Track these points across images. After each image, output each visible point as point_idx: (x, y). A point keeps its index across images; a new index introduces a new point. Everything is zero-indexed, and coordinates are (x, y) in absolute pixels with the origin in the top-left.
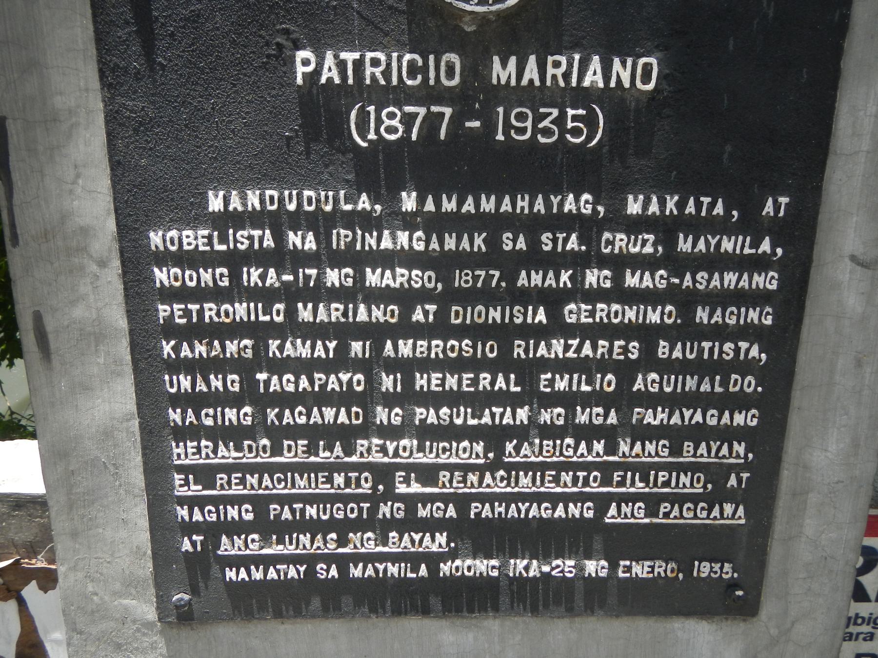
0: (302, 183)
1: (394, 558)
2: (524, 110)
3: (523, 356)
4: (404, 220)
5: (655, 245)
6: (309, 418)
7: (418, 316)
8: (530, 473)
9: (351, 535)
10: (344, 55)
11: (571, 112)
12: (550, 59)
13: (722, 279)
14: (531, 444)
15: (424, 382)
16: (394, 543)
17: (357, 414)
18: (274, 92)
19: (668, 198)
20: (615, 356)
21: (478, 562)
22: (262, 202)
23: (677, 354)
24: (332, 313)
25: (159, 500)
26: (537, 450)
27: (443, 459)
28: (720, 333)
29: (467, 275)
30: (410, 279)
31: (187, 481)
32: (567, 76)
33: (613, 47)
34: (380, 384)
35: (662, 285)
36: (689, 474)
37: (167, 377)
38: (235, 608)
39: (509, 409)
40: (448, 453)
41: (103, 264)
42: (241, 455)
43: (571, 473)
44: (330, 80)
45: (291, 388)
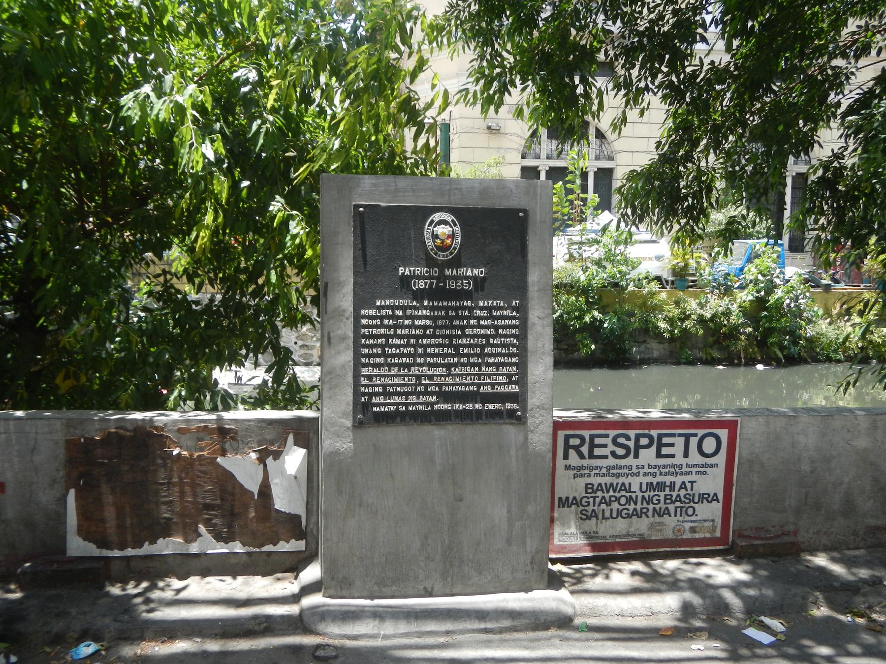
7: (428, 332)
24: (407, 331)
25: (357, 385)
28: (506, 336)
33: (473, 267)
41: (347, 319)
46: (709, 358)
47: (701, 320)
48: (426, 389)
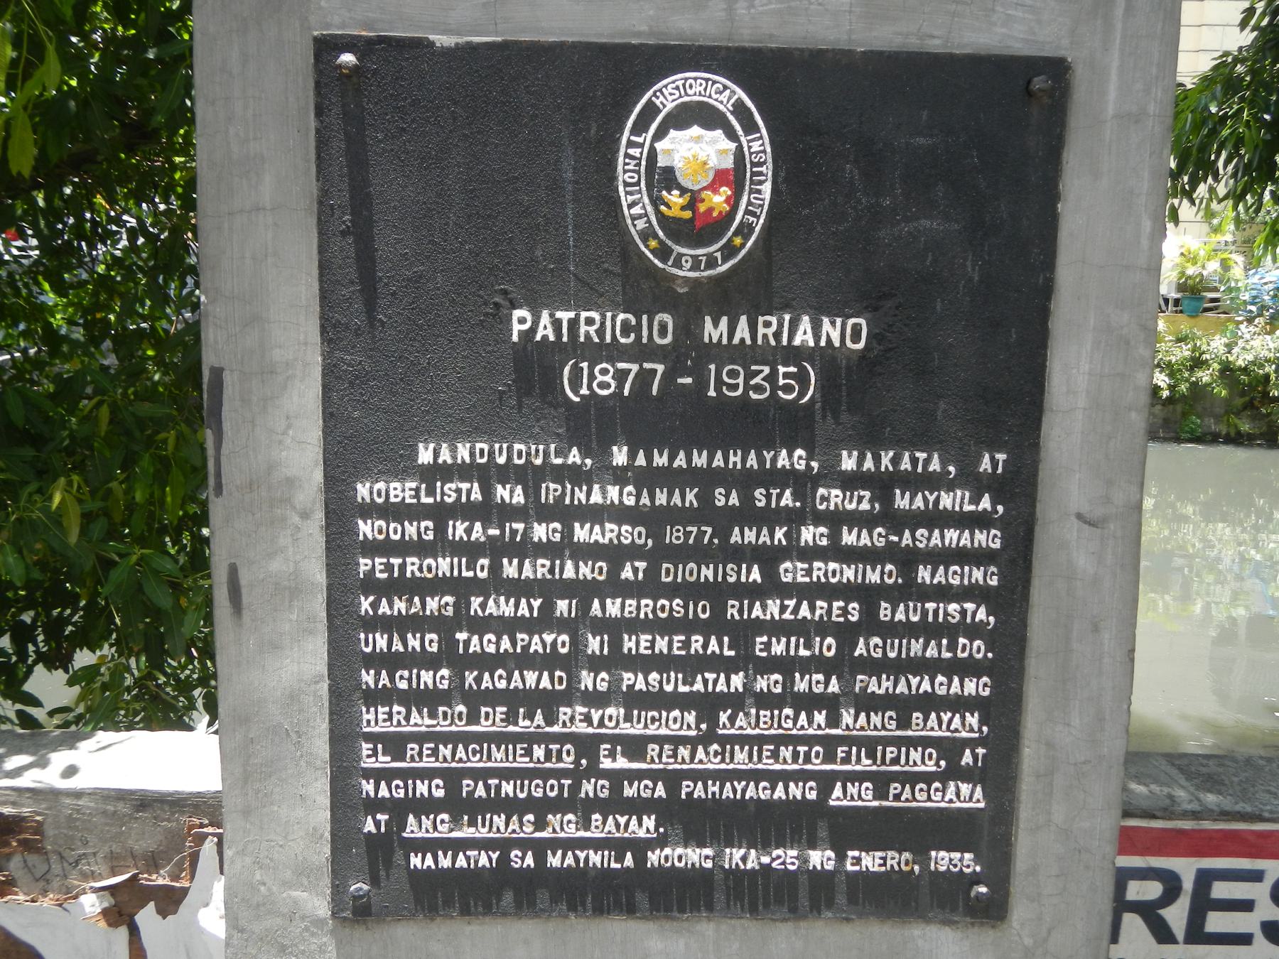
0: (511, 437)
1: (597, 845)
2: (736, 367)
3: (737, 617)
4: (614, 474)
5: (871, 501)
6: (509, 683)
7: (627, 573)
8: (747, 748)
9: (550, 816)
10: (559, 314)
11: (782, 370)
12: (761, 319)
13: (942, 537)
14: (747, 715)
15: (632, 645)
16: (597, 827)
17: (561, 678)
18: (490, 348)
19: (883, 454)
20: (834, 618)
21: (689, 851)
22: (472, 454)
23: (900, 616)
24: (537, 569)
26: (753, 721)
27: (652, 730)
28: (944, 593)
29: (678, 531)
30: (620, 534)
31: (375, 751)
32: (777, 335)
33: (821, 308)
34: (586, 646)
35: (881, 543)
36: (920, 749)
37: (362, 636)
38: (418, 901)
39: (722, 675)
40: (657, 723)
41: (305, 515)
42: (435, 722)
43: (791, 748)
44: (545, 337)
45: (491, 649)
46: (1233, 434)
47: (1227, 371)
48: (616, 788)
